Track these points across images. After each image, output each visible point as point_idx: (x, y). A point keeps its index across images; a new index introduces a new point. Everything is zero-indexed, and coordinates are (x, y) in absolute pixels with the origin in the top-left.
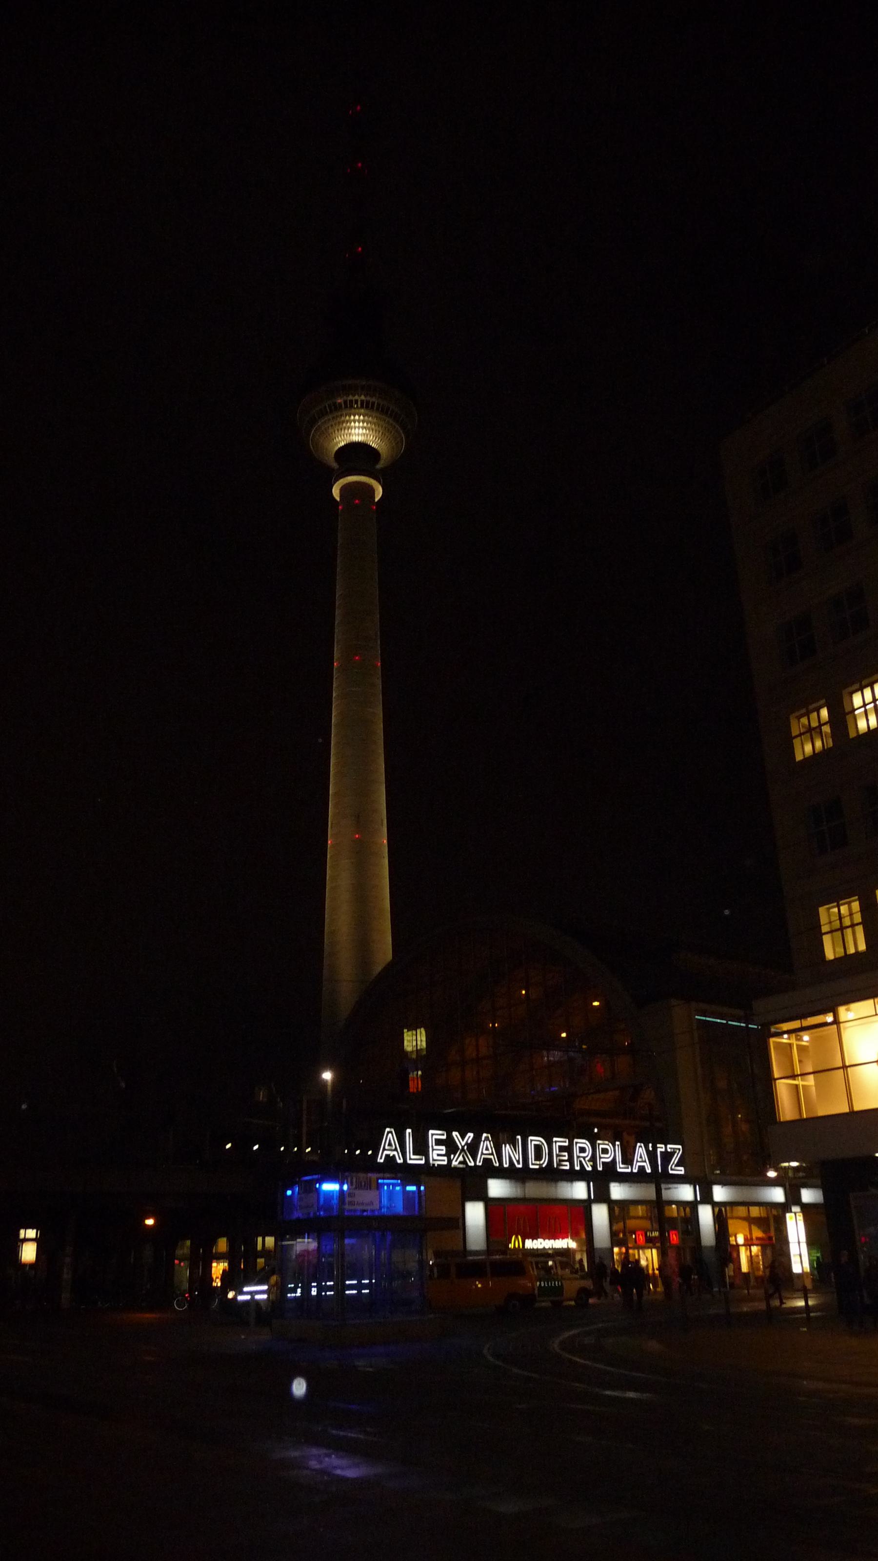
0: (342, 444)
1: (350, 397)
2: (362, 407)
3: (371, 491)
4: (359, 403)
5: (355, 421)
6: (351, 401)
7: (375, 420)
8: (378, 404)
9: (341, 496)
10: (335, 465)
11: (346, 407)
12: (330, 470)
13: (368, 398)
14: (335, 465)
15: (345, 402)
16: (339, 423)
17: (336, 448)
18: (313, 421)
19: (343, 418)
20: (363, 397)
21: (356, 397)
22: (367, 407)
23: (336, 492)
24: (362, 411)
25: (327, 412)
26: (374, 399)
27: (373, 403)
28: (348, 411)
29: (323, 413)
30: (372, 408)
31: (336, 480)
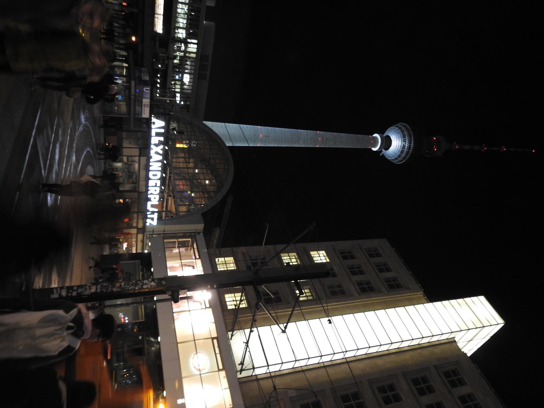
0: (392, 138)
1: (407, 141)
2: (404, 145)
3: (375, 147)
4: (405, 144)
5: (399, 142)
6: (406, 141)
7: (399, 149)
8: (404, 151)
9: (374, 137)
10: (385, 135)
11: (404, 140)
12: (383, 133)
13: (406, 147)
14: (385, 135)
15: (406, 139)
16: (399, 137)
17: (390, 136)
18: (400, 128)
19: (400, 138)
20: (407, 146)
21: (407, 143)
22: (403, 147)
23: (376, 135)
24: (402, 145)
25: (403, 133)
26: (406, 149)
27: (405, 149)
28: (403, 140)
29: (402, 131)
30: (403, 149)
31: (380, 135)
